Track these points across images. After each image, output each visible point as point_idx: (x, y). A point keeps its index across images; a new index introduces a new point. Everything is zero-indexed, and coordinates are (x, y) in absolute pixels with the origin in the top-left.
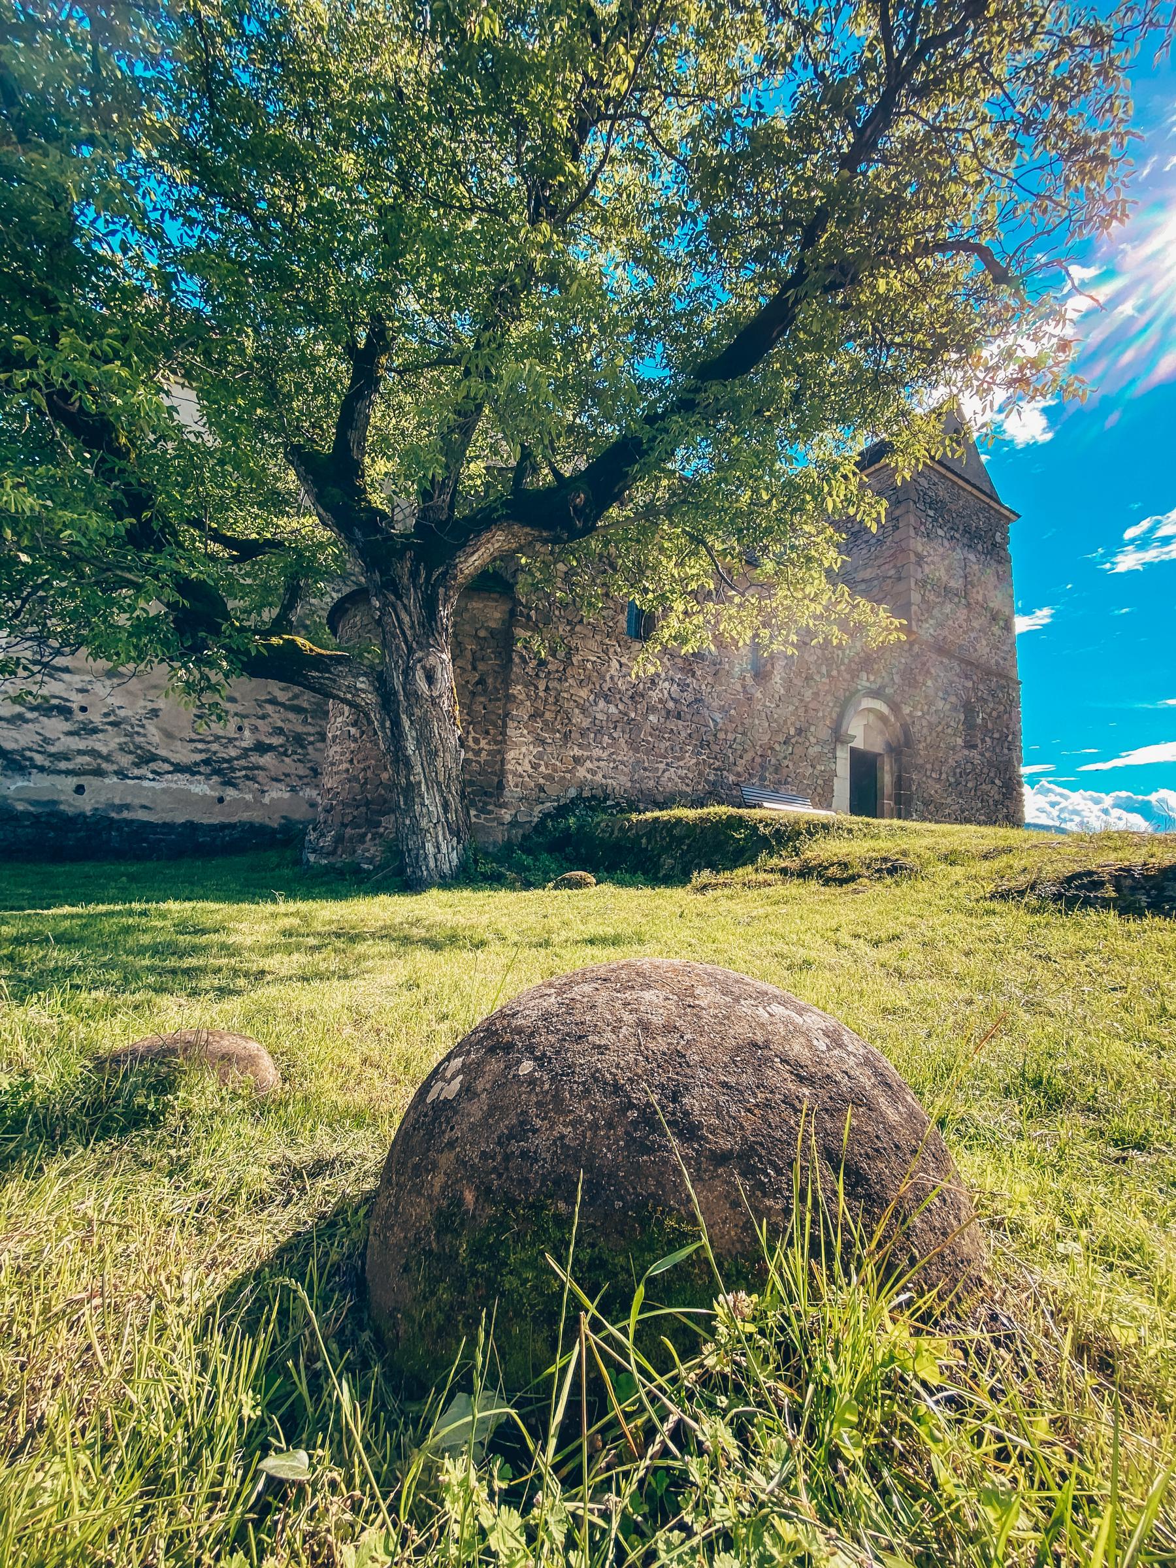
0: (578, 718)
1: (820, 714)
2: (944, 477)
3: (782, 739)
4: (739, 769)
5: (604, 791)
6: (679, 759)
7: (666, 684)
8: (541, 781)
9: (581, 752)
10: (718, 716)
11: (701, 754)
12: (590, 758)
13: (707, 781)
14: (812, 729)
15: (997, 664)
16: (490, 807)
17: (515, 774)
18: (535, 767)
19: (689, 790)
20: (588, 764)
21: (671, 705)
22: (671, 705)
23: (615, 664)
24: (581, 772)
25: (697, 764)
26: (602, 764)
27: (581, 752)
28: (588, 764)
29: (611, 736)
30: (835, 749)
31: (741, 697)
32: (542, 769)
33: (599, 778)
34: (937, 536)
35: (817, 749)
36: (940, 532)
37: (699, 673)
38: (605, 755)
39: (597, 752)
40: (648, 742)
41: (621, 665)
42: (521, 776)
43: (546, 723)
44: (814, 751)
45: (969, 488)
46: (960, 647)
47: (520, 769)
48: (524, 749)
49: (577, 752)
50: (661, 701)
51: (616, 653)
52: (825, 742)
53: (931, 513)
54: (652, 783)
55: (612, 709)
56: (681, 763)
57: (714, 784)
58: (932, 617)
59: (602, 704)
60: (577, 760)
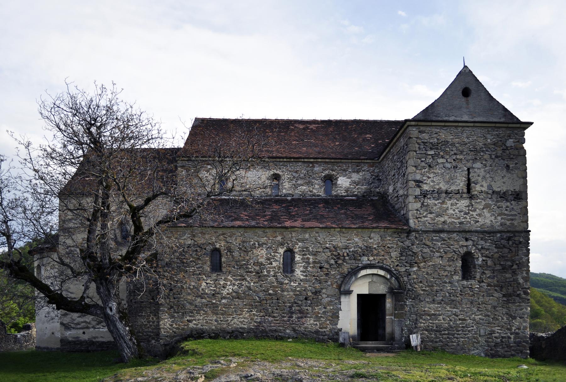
0: (188, 306)
1: (329, 283)
2: (445, 126)
3: (301, 298)
4: (275, 315)
5: (202, 331)
6: (240, 315)
7: (231, 287)
8: (174, 330)
9: (190, 318)
10: (261, 294)
11: (252, 311)
12: (195, 320)
13: (255, 322)
14: (324, 291)
15: (502, 224)
16: (159, 340)
17: (164, 328)
18: (171, 325)
19: (245, 326)
20: (194, 322)
21: (234, 294)
22: (234, 294)
23: (204, 284)
24: (191, 325)
25: (250, 316)
26: (200, 321)
27: (190, 318)
28: (194, 322)
29: (204, 311)
30: (340, 298)
31: (275, 284)
32: (174, 326)
33: (199, 326)
34: (438, 164)
35: (329, 299)
36: (441, 161)
37: (248, 279)
38: (201, 318)
39: (198, 317)
40: (223, 310)
41: (207, 284)
42: (166, 329)
43: (174, 310)
44: (326, 300)
45: (472, 125)
46: (461, 223)
47: (165, 327)
48: (166, 320)
49: (188, 318)
50: (228, 294)
51: (204, 280)
52: (332, 296)
53: (432, 152)
54: (225, 326)
55: (204, 300)
56: (241, 316)
57: (260, 323)
58: (431, 213)
59: (199, 300)
60: (189, 321)
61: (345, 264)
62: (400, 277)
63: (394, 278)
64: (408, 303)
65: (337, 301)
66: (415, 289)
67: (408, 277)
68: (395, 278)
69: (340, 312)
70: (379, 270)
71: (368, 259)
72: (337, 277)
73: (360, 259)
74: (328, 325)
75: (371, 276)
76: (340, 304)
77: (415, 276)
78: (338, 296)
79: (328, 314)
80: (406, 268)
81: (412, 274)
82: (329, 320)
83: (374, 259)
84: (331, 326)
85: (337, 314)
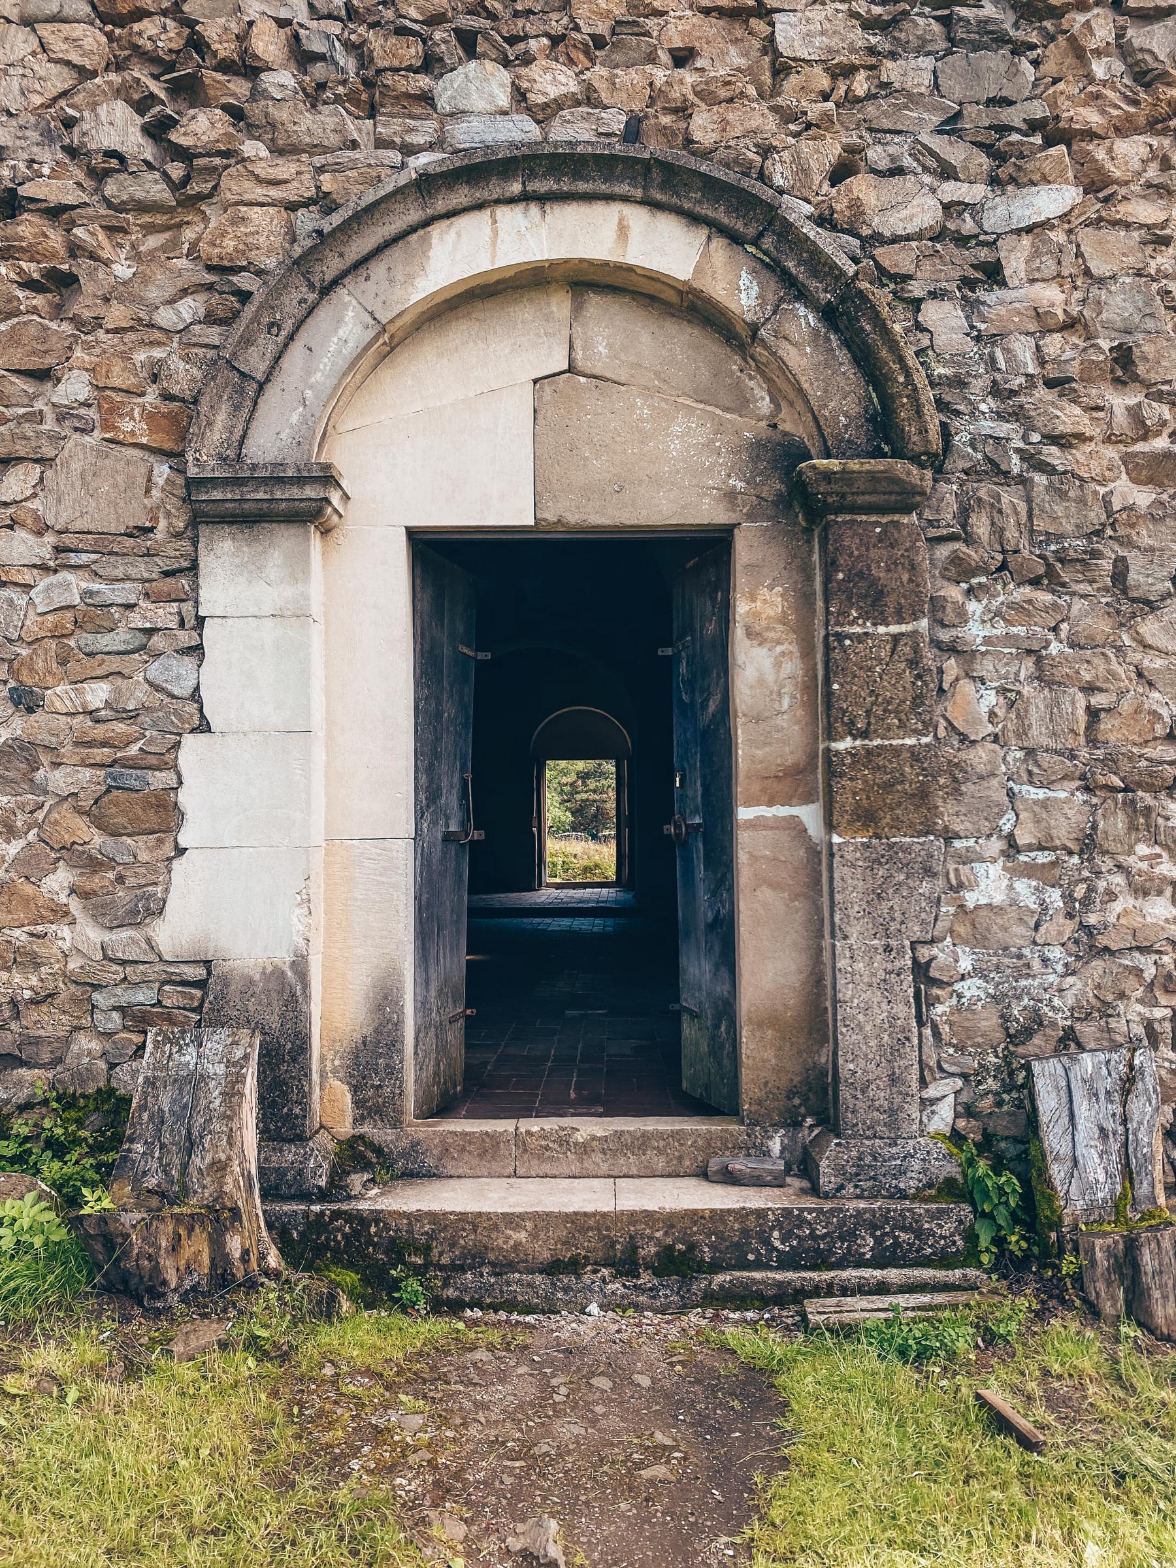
61: (252, 148)
62: (882, 296)
63: (805, 318)
64: (975, 632)
65: (164, 615)
66: (1053, 454)
67: (971, 306)
68: (828, 315)
69: (192, 751)
70: (637, 216)
71: (520, 95)
72: (165, 317)
73: (427, 98)
74: (61, 913)
75: (560, 305)
76: (196, 651)
77: (1051, 296)
78: (173, 554)
79: (59, 780)
80: (951, 191)
81: (1015, 263)
82: (68, 852)
83: (589, 98)
84: (92, 934)
85: (160, 779)
